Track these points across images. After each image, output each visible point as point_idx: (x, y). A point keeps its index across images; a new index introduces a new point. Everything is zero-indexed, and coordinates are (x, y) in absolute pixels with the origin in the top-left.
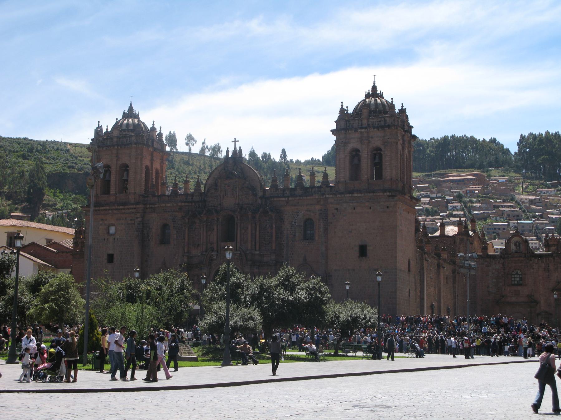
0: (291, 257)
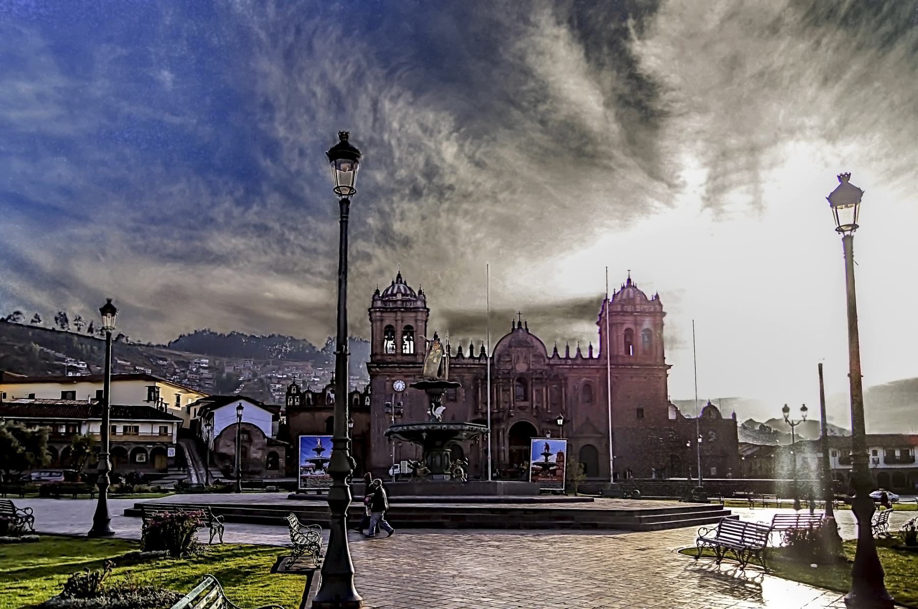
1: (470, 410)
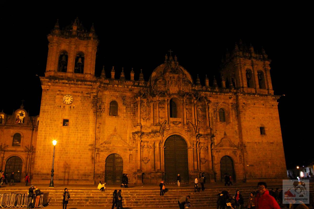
0: (216, 132)
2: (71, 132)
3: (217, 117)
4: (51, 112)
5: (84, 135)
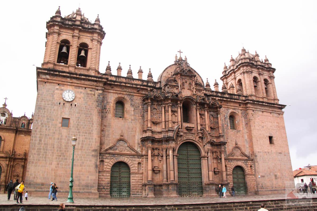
1: (138, 127)
2: (72, 135)
3: (228, 124)
4: (48, 110)
5: (86, 138)
